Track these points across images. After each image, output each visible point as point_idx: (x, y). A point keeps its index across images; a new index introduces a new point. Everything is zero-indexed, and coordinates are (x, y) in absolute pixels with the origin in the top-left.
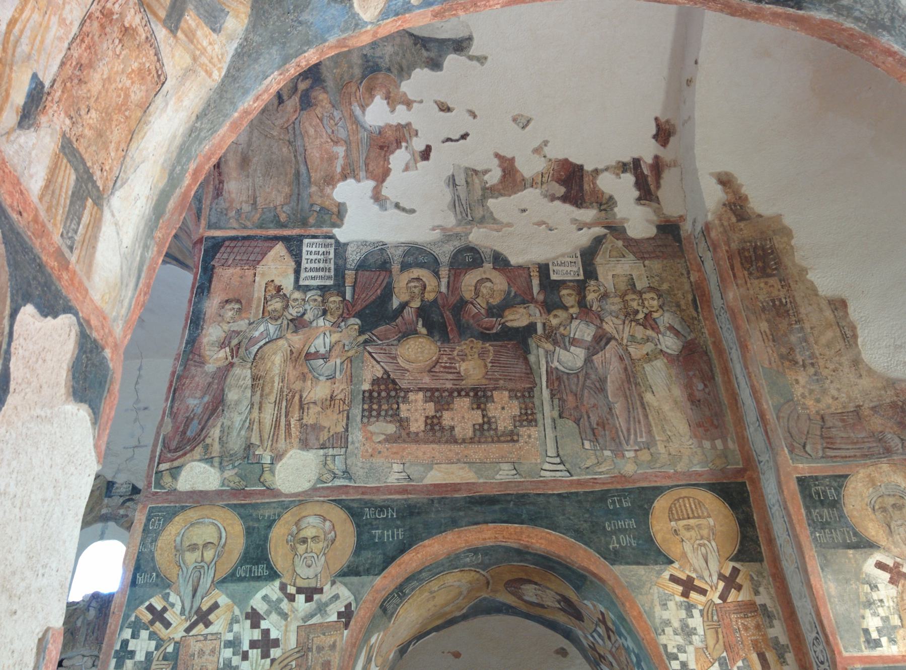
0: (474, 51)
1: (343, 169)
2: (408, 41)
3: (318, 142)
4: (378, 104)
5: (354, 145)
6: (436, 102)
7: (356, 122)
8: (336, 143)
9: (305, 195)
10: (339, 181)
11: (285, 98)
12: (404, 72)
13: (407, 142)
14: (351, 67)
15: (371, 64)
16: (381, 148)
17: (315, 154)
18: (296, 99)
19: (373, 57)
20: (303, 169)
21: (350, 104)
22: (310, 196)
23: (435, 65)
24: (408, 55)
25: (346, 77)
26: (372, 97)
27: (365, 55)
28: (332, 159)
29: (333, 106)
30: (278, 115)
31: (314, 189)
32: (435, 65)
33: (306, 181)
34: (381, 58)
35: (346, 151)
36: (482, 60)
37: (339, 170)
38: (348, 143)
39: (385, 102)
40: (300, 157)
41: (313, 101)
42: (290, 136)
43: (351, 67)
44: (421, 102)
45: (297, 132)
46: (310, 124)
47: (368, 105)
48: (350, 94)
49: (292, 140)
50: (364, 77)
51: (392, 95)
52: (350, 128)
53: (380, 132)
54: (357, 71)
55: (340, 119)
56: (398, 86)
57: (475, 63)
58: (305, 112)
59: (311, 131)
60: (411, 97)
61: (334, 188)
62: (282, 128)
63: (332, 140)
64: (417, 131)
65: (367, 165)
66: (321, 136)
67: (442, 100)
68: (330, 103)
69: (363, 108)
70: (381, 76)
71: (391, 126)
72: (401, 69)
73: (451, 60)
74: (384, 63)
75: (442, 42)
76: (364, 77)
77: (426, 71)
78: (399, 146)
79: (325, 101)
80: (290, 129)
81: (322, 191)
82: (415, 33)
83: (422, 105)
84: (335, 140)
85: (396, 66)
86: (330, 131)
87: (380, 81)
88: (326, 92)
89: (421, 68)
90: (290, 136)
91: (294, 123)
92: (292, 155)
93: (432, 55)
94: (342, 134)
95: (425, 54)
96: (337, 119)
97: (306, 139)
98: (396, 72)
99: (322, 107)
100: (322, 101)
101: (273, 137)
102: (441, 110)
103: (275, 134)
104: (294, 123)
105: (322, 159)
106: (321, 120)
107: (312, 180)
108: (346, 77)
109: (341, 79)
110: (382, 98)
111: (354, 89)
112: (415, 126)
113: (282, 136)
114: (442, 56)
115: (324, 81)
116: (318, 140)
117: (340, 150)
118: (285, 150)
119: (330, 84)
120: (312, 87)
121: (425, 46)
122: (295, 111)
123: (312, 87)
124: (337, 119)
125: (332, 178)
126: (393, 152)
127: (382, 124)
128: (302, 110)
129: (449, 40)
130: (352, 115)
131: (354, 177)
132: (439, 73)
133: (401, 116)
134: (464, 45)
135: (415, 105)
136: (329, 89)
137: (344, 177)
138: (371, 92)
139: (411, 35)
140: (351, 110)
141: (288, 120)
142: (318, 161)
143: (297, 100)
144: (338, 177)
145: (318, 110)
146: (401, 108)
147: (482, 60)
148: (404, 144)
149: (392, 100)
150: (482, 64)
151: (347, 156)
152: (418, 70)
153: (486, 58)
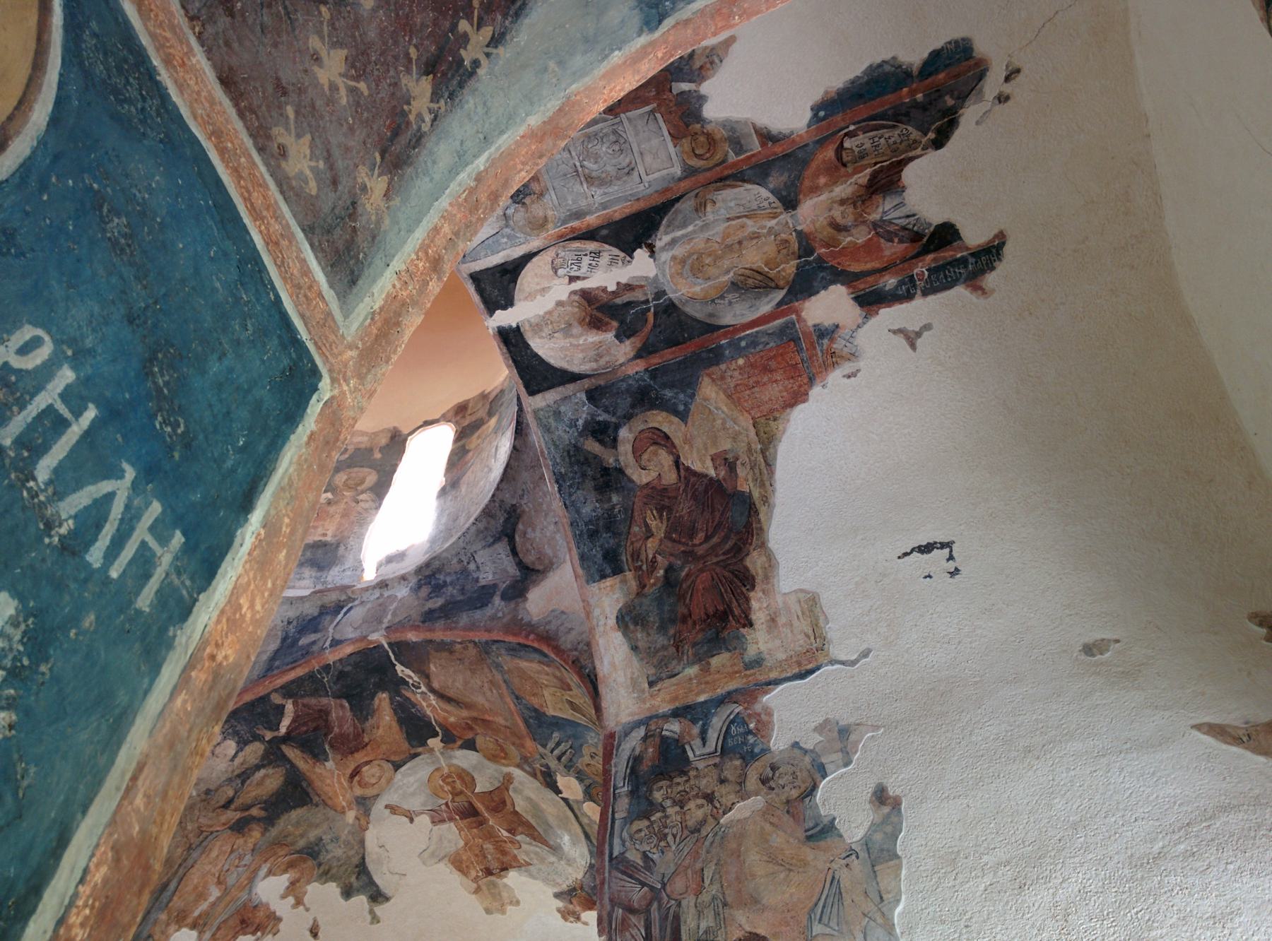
0: (379, 910)
1: (200, 916)
2: (356, 860)
3: (207, 868)
4: (283, 880)
5: (228, 898)
6: (315, 920)
7: (251, 880)
8: (219, 882)
9: (153, 916)
10: (186, 926)
11: (233, 807)
12: (326, 876)
13: (263, 934)
14: (302, 836)
15: (316, 848)
16: (243, 922)
17: (195, 877)
18: (238, 815)
19: (324, 845)
20: (172, 886)
21: (265, 861)
22: (156, 922)
23: (347, 893)
24: (343, 868)
25: (289, 839)
26: (285, 871)
27: (321, 839)
28: (201, 896)
29: (253, 850)
30: (210, 814)
31: (163, 917)
32: (347, 893)
33: (165, 901)
34: (327, 851)
35: (218, 898)
36: (375, 919)
37: (196, 913)
38: (226, 892)
39: (287, 884)
40: (178, 868)
41: (246, 830)
42: (197, 841)
43: (302, 836)
44: (307, 910)
45: (204, 844)
46: (221, 846)
47: (274, 875)
48: (275, 854)
49: (194, 846)
50: (298, 852)
51: (298, 885)
52: (242, 880)
53: (255, 907)
54: (301, 843)
55: (245, 865)
56: (309, 882)
57: (369, 918)
58: (229, 832)
59: (214, 854)
60: (306, 899)
61: (177, 930)
62: (199, 828)
63: (219, 878)
64: (278, 931)
65: (219, 928)
66: (216, 865)
67: (320, 923)
68: (255, 845)
69: (270, 873)
70: (310, 863)
71: (268, 909)
72: (326, 873)
73: (361, 900)
74: (324, 857)
75: (372, 883)
76: (298, 852)
77: (338, 891)
78: (253, 933)
79: (253, 840)
80: (205, 834)
81: (168, 925)
82: (367, 860)
83: (305, 912)
84: (222, 878)
85: (327, 868)
86: (226, 867)
87: (305, 866)
88: (263, 834)
89: (337, 886)
90: (195, 841)
91: (212, 833)
92: (179, 861)
93: (356, 884)
94: (231, 880)
95: (353, 879)
96: (243, 863)
97: (204, 856)
98: (321, 871)
99: (245, 841)
100: (251, 837)
101: (185, 829)
102: (311, 931)
103: (189, 828)
104: (212, 833)
105: (196, 888)
106: (232, 851)
107: (171, 904)
108: (289, 839)
109: (286, 836)
110: (288, 879)
111: (283, 853)
112: (282, 926)
113: (191, 835)
114: (359, 891)
115: (273, 825)
116: (210, 866)
117: (215, 893)
118: (179, 850)
119: (274, 832)
120: (259, 820)
121: (359, 874)
122: (224, 824)
123: (259, 820)
124: (243, 863)
125: (185, 918)
126: (245, 934)
127: (264, 900)
128: (230, 828)
129: (377, 886)
130: (255, 872)
131: (200, 933)
132: (342, 901)
133: (282, 907)
134: (380, 899)
135: (301, 908)
136: (267, 834)
137: (193, 926)
138: (290, 866)
139: (363, 858)
140: (260, 866)
141: (211, 826)
142: (190, 888)
143: (238, 817)
144: (189, 920)
145: (240, 841)
146: (291, 900)
147: (375, 919)
148: (259, 934)
149: (294, 891)
150: (372, 923)
151: (213, 905)
152: (334, 884)
153: (378, 922)
